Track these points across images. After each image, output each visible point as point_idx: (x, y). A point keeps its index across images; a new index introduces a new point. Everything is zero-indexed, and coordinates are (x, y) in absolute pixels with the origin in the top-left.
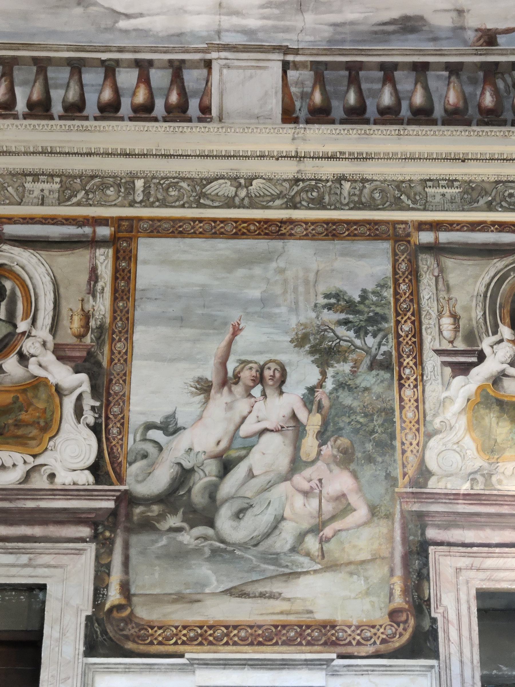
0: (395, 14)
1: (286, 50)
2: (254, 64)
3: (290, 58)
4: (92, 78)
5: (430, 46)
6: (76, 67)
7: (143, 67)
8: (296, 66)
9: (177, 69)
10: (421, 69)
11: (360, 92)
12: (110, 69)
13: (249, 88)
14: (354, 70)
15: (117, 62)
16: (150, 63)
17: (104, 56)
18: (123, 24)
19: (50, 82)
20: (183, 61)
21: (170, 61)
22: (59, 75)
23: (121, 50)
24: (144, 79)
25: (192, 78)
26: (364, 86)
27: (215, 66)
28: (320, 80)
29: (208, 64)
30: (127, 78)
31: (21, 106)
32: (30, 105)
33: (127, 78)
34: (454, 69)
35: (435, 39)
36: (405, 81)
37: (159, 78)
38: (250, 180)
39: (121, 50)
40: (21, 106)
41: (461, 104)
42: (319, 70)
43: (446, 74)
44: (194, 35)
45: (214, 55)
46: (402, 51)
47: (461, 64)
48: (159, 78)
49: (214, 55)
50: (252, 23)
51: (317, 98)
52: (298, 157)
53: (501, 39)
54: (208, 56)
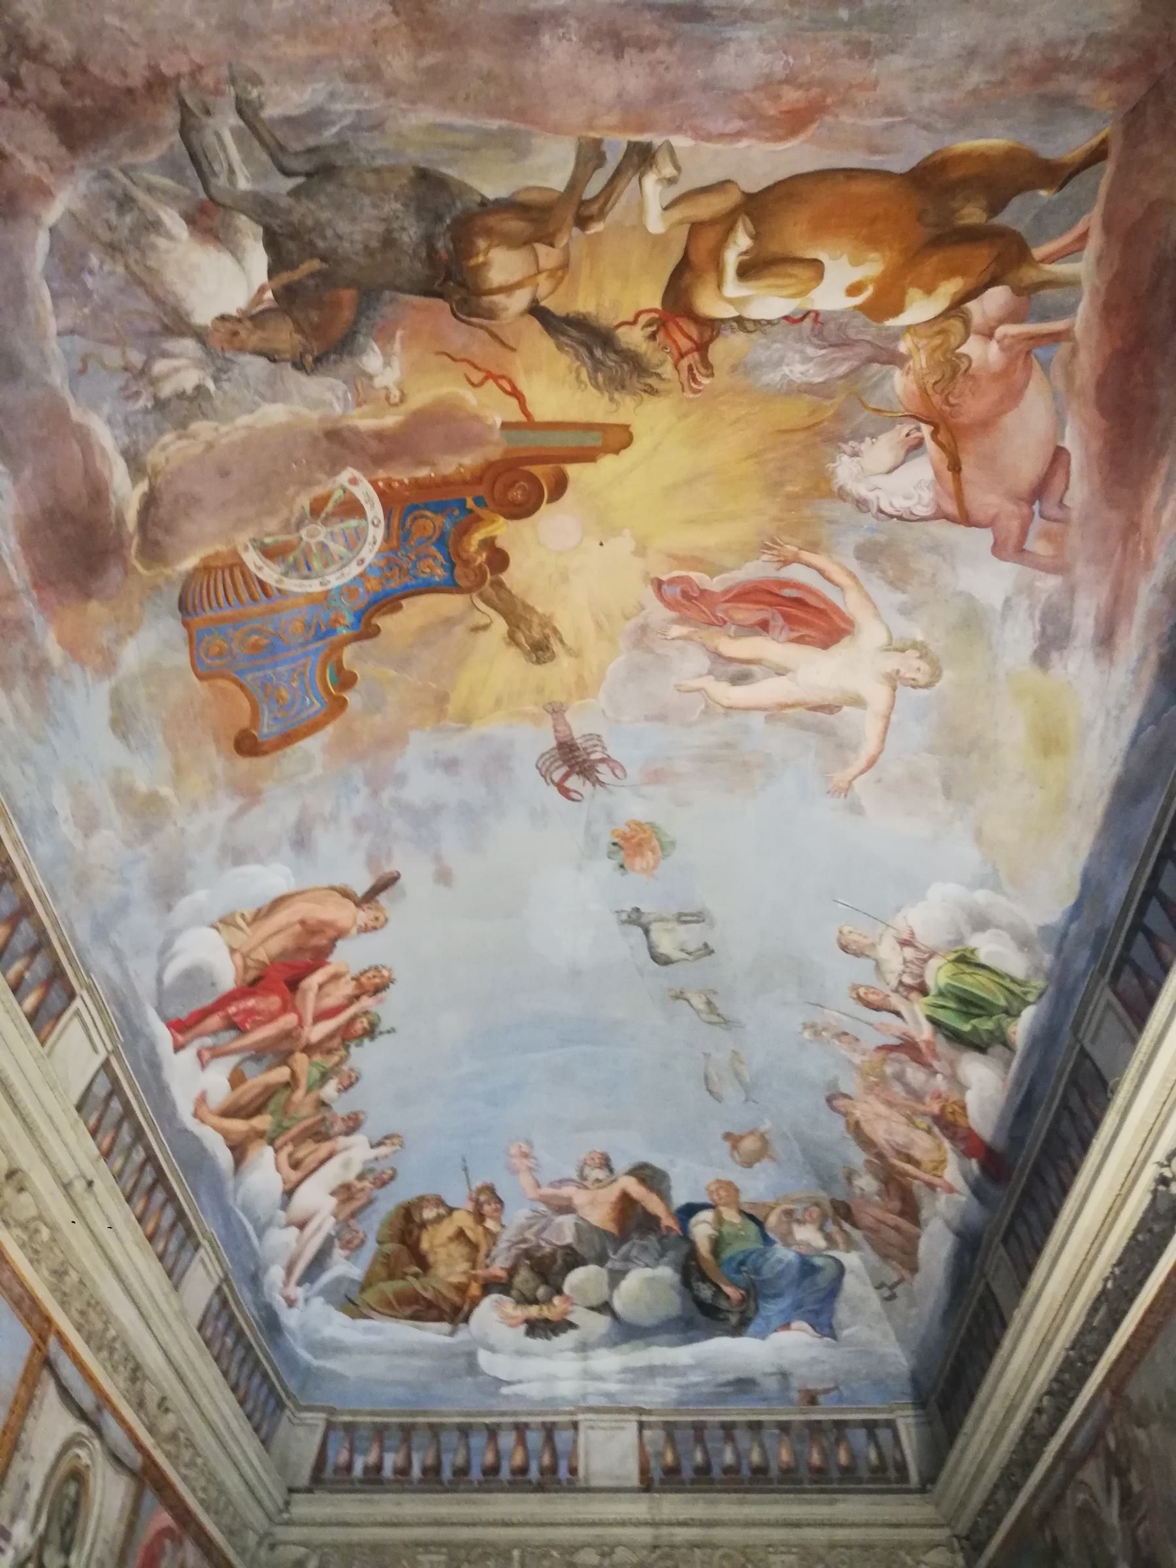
0: (731, 1377)
1: (640, 1411)
2: (614, 1424)
3: (644, 1418)
4: (478, 1441)
5: (762, 1406)
6: (464, 1430)
7: (521, 1429)
8: (650, 1425)
9: (549, 1430)
10: (755, 1427)
11: (706, 1452)
12: (492, 1432)
13: (609, 1451)
14: (699, 1428)
15: (499, 1425)
16: (526, 1426)
17: (488, 1420)
18: (505, 1390)
19: (443, 1447)
20: (554, 1424)
21: (544, 1424)
22: (450, 1439)
23: (503, 1414)
24: (522, 1441)
25: (562, 1438)
26: (709, 1445)
27: (581, 1427)
28: (671, 1439)
29: (575, 1425)
30: (507, 1440)
31: (416, 1472)
32: (425, 1470)
33: (507, 1440)
34: (784, 1427)
35: (764, 1399)
36: (743, 1438)
37: (535, 1439)
38: (613, 1548)
39: (503, 1414)
40: (416, 1472)
41: (792, 1464)
42: (669, 1428)
43: (777, 1431)
44: (564, 1399)
45: (580, 1417)
46: (738, 1412)
47: (788, 1422)
48: (535, 1439)
49: (580, 1417)
50: (613, 1387)
51: (669, 1458)
52: (653, 1524)
53: (821, 1399)
54: (575, 1418)
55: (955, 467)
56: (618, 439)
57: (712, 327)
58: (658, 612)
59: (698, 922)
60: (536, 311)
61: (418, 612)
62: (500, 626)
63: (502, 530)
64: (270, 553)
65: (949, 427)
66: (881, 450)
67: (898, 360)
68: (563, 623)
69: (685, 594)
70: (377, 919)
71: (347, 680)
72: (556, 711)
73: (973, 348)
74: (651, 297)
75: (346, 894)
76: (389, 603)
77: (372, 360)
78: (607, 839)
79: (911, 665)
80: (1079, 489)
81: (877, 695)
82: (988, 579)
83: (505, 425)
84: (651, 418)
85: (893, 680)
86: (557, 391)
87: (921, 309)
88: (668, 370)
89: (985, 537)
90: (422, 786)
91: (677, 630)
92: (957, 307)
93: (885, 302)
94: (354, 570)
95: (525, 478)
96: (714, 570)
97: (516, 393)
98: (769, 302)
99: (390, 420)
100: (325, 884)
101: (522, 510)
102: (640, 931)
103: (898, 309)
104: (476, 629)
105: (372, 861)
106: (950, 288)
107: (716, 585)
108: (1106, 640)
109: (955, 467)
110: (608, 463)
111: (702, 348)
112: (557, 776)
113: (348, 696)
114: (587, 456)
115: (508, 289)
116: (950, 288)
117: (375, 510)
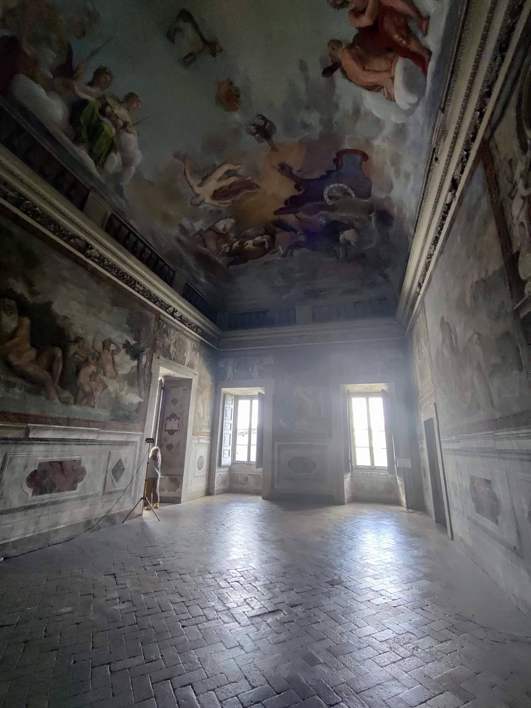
55: (216, 232)
56: (276, 213)
57: (266, 233)
58: (255, 181)
59: (186, 57)
60: (296, 232)
61: (316, 175)
62: (294, 171)
63: (297, 193)
64: (349, 194)
65: (222, 236)
66: (229, 226)
67: (234, 237)
68: (279, 174)
69: (251, 187)
70: (333, 49)
71: (335, 161)
72: (274, 149)
73: (226, 245)
74: (278, 236)
75: (344, 72)
76: (322, 178)
77: (324, 222)
78: (242, 98)
79: (197, 201)
80: (200, 247)
81: (198, 190)
82: (199, 225)
83: (299, 212)
84: (271, 217)
85: (198, 195)
86: (290, 218)
87: (236, 244)
88: (271, 226)
89: (204, 229)
90: (314, 118)
91: (249, 178)
92: (231, 247)
93: (242, 244)
94: (331, 186)
95: (292, 204)
96: (247, 194)
97: (297, 218)
98: (258, 239)
99: (322, 212)
100: (352, 84)
101: (292, 198)
102: (206, 37)
103: (239, 243)
104: (300, 171)
105: (332, 86)
106: (234, 248)
107: (245, 191)
108: (179, 241)
109: (216, 232)
110: (277, 208)
111: (266, 229)
112: (268, 124)
113: (335, 157)
114: (281, 209)
115: (301, 234)
116: (234, 248)
117: (325, 196)
